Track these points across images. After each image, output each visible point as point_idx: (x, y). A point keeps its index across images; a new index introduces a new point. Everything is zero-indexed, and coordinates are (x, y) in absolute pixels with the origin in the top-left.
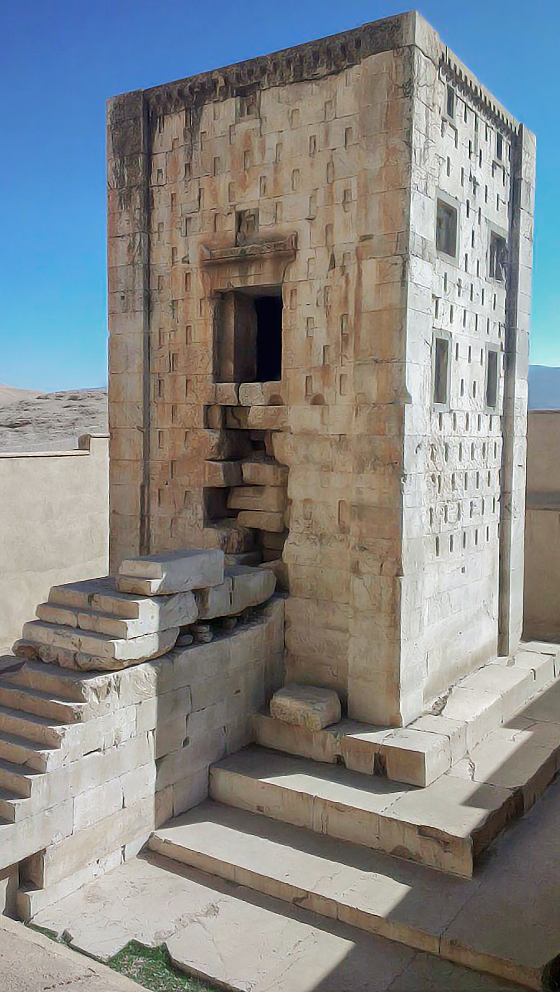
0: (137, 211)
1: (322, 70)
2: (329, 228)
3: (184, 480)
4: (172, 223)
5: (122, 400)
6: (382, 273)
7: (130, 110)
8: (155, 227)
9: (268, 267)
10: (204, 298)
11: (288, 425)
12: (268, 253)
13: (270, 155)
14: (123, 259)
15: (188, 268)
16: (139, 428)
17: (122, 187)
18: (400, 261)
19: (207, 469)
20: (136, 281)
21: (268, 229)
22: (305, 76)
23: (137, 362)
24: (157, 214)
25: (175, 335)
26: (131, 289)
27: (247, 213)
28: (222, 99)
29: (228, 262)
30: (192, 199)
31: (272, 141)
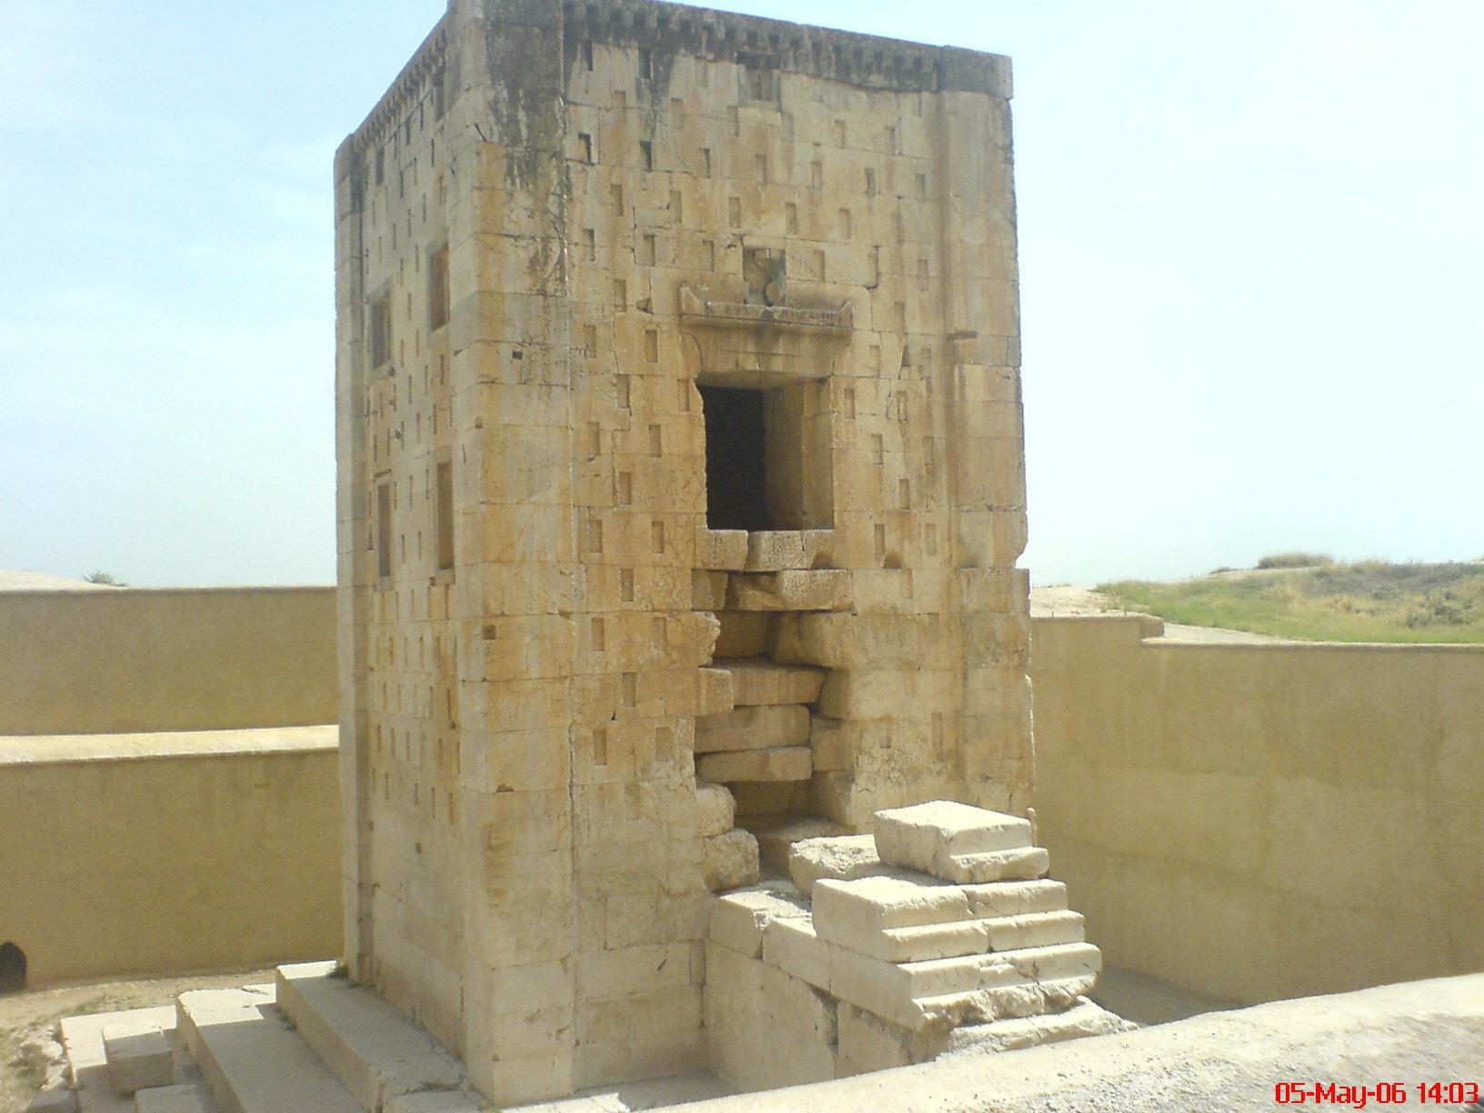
1: (876, 80)
2: (901, 306)
8: (575, 234)
9: (806, 346)
11: (850, 600)
12: (811, 325)
13: (802, 175)
14: (516, 282)
15: (651, 322)
18: (1012, 375)
19: (704, 684)
22: (855, 78)
23: (556, 484)
24: (578, 211)
27: (760, 255)
28: (711, 56)
29: (738, 328)
30: (657, 203)
31: (804, 153)
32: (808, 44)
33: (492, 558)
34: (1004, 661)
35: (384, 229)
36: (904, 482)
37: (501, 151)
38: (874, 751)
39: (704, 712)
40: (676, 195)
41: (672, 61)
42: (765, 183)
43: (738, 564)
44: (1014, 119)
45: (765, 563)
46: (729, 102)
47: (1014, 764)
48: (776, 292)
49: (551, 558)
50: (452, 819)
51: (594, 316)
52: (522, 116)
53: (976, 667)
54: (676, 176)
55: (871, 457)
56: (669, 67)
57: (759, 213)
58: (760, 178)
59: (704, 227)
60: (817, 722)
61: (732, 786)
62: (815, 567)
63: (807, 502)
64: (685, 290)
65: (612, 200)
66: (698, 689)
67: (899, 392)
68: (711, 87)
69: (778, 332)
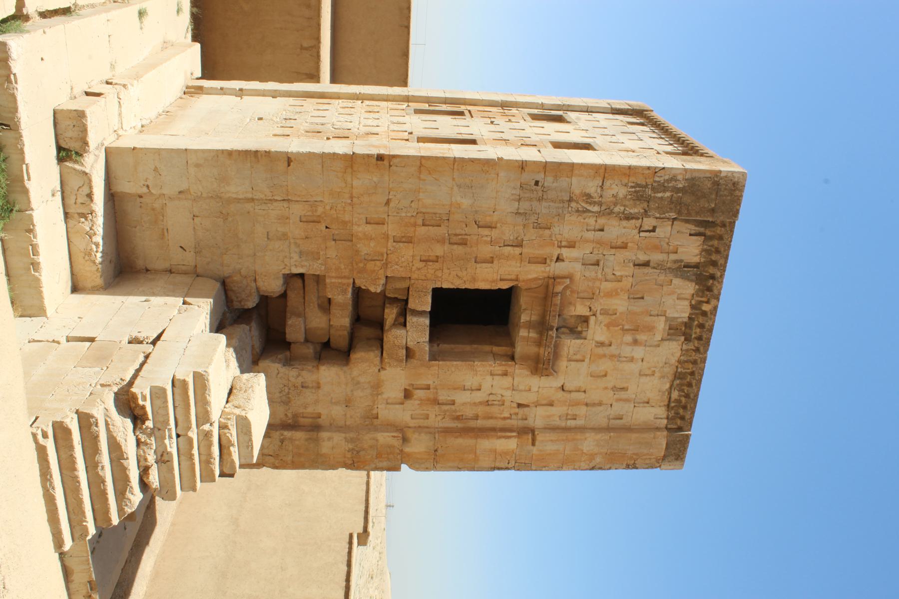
0: (622, 208)
1: (675, 395)
2: (551, 404)
3: (332, 253)
4: (600, 243)
5: (422, 176)
6: (504, 454)
7: (724, 203)
8: (602, 221)
9: (532, 350)
10: (517, 280)
12: (544, 352)
13: (627, 351)
16: (388, 203)
17: (653, 189)
18: (510, 466)
19: (345, 281)
20: (551, 204)
21: (566, 349)
25: (486, 242)
26: (545, 197)
28: (693, 302)
31: (639, 352)
32: (697, 356)
33: (423, 161)
34: (349, 455)
35: (603, 123)
36: (453, 403)
37: (650, 181)
38: (300, 378)
39: (328, 281)
40: (619, 280)
41: (691, 281)
42: (623, 329)
43: (411, 305)
44: (650, 471)
45: (411, 320)
46: (668, 311)
47: (290, 458)
48: (563, 333)
49: (421, 195)
50: (275, 135)
51: (556, 230)
52: (668, 194)
53: (345, 438)
54: (630, 279)
55: (468, 384)
56: (688, 279)
57: (608, 326)
58: (626, 327)
59: (602, 294)
60: (318, 348)
61: (284, 296)
62: (407, 349)
63: (445, 347)
64: (568, 281)
65: (619, 243)
66: (342, 278)
67: (504, 401)
68: (677, 302)
69: (541, 333)
